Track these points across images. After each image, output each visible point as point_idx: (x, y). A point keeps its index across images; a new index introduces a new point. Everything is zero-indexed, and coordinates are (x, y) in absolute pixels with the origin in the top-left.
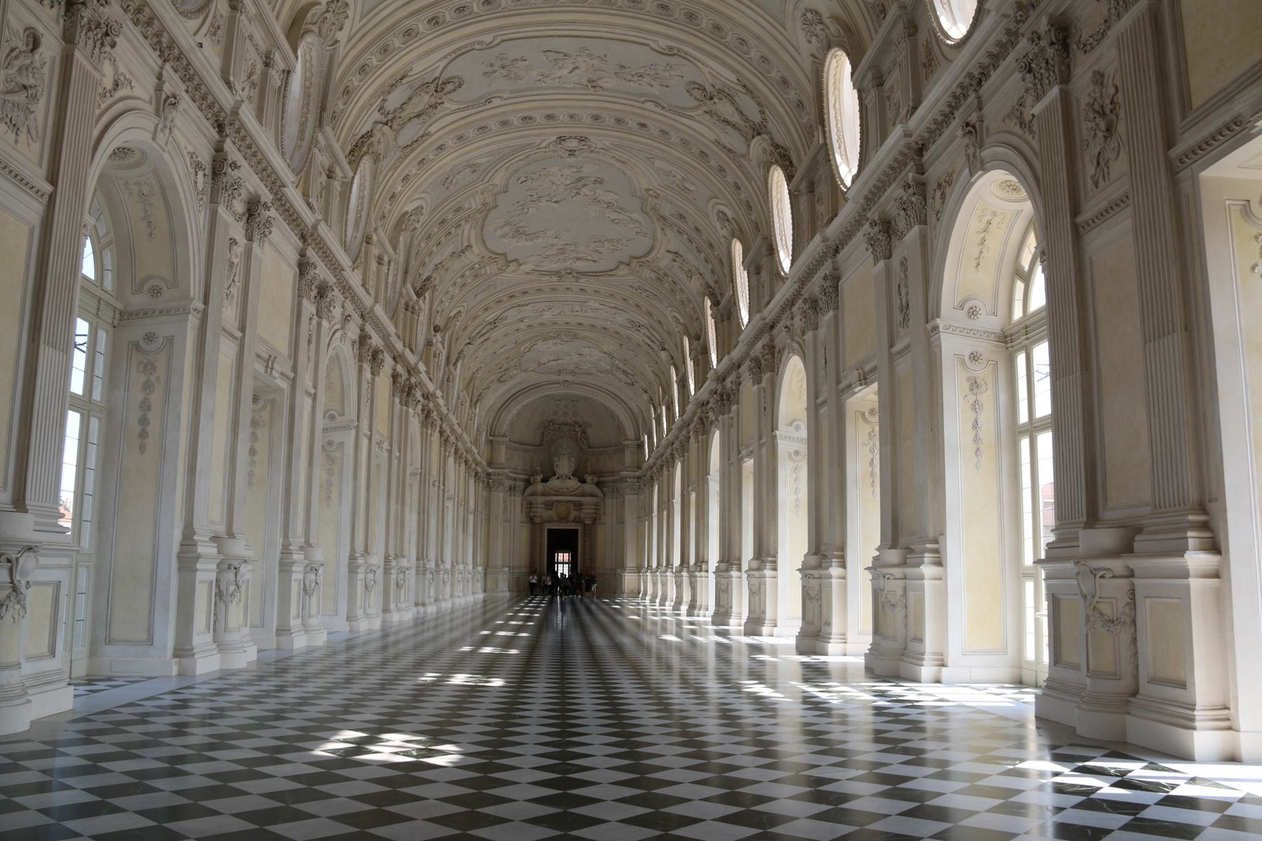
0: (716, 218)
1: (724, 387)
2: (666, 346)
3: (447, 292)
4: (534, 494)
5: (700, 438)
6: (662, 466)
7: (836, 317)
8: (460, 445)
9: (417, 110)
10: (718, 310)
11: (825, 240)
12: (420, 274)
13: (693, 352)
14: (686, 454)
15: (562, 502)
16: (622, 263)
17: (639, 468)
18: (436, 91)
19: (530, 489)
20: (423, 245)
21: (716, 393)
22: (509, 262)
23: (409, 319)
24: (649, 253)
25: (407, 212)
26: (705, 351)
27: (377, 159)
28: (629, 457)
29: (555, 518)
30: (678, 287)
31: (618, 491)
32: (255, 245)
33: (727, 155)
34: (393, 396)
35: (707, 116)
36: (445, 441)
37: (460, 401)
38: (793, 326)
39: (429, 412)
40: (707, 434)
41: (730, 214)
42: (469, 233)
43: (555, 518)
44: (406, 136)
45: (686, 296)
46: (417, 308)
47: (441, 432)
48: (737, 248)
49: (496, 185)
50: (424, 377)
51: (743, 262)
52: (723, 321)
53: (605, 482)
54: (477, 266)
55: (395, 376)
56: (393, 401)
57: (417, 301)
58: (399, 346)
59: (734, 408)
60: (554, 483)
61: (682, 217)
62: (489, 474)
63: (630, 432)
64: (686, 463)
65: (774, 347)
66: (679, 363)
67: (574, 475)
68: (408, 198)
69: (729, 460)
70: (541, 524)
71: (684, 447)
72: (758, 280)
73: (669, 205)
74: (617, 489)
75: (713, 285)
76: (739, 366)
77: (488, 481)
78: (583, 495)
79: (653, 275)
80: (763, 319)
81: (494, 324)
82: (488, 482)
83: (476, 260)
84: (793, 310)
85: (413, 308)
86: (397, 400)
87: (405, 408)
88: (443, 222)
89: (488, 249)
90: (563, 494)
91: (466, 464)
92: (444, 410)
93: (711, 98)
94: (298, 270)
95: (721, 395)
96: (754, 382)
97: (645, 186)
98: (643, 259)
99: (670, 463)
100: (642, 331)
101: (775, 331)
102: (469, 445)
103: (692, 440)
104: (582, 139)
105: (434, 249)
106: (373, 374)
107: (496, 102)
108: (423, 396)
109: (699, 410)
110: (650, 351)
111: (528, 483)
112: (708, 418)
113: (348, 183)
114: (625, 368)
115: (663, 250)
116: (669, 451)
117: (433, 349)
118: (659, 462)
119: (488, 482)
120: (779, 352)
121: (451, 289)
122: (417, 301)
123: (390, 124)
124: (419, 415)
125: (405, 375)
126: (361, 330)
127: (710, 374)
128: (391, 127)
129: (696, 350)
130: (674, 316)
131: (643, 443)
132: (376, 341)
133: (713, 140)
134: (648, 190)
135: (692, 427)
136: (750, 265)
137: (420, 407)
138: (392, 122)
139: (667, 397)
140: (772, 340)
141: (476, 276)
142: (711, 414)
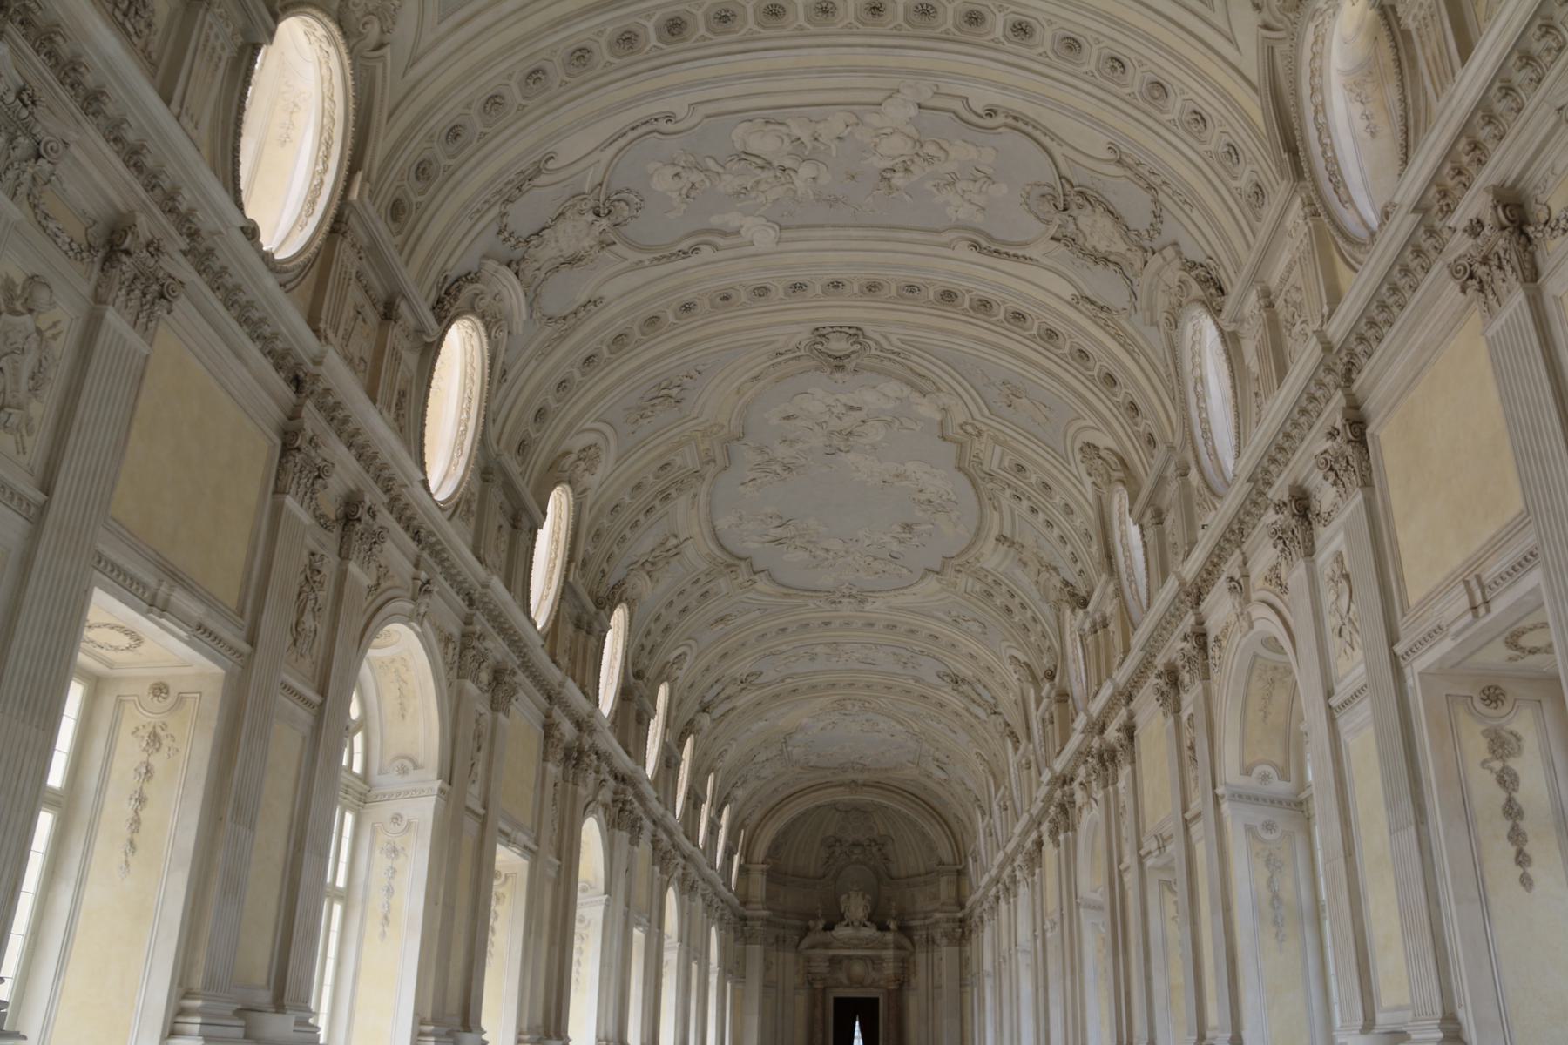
0: (1079, 456)
1: (1103, 740)
2: (1000, 709)
3: (658, 618)
4: (813, 947)
5: (1061, 837)
6: (998, 898)
7: (1369, 504)
8: (691, 870)
9: (568, 252)
10: (1086, 613)
11: (1327, 347)
12: (603, 571)
13: (1045, 702)
14: (1037, 871)
15: (849, 957)
16: (929, 570)
17: (962, 906)
18: (598, 215)
19: (806, 942)
20: (606, 522)
21: (1089, 754)
22: (755, 573)
23: (581, 639)
24: (968, 548)
25: (567, 453)
26: (1063, 697)
27: (492, 322)
28: (945, 888)
29: (845, 981)
30: (1017, 600)
31: (934, 942)
32: (115, 320)
33: (1093, 319)
34: (545, 760)
35: (1059, 249)
36: (661, 857)
37: (692, 801)
38: (1246, 576)
39: (624, 803)
40: (1074, 830)
41: (1104, 440)
42: (684, 516)
43: (845, 981)
44: (553, 302)
45: (1029, 614)
46: (596, 626)
47: (655, 842)
48: (1119, 500)
49: (723, 427)
50: (609, 742)
51: (1130, 511)
52: (1096, 632)
53: (916, 927)
54: (703, 580)
55: (549, 728)
56: (544, 770)
57: (597, 614)
58: (554, 674)
59: (1125, 772)
60: (841, 932)
61: (1021, 468)
62: (744, 919)
63: (946, 853)
64: (1037, 888)
65: (1204, 635)
66: (1020, 733)
67: (869, 920)
68: (571, 425)
69: (1120, 862)
70: (824, 989)
71: (1035, 857)
72: (1161, 536)
73: (998, 449)
74: (933, 938)
75: (1071, 579)
76: (1130, 699)
77: (739, 927)
78: (885, 947)
79: (978, 587)
80: (1182, 584)
81: (745, 682)
82: (743, 931)
83: (704, 566)
84: (1245, 547)
85: (590, 624)
86: (554, 770)
87: (570, 786)
88: (638, 486)
89: (722, 547)
90: (856, 947)
91: (704, 900)
92: (657, 808)
93: (1065, 209)
94: (279, 442)
95: (1101, 756)
96: (1165, 714)
97: (960, 418)
98: (963, 560)
99: (1010, 890)
100: (961, 689)
101: (1203, 605)
102: (709, 871)
103: (1048, 847)
104: (855, 333)
105: (627, 532)
106: (495, 707)
107: (706, 252)
108: (616, 778)
109: (1058, 793)
110: (975, 722)
111: (807, 930)
112: (1074, 803)
113: (432, 344)
114: (937, 754)
115: (992, 541)
116: (1008, 870)
117: (634, 706)
118: (994, 891)
119: (743, 931)
120: (1217, 640)
121: (663, 611)
122: (597, 614)
123: (514, 265)
124: (605, 806)
125: (567, 729)
126: (466, 624)
127: (1080, 722)
128: (517, 274)
129: (1048, 697)
130: (1013, 657)
131: (966, 867)
132: (496, 647)
133: (1069, 298)
134: (961, 427)
135: (1045, 827)
136: (1142, 515)
137: (606, 795)
138: (518, 264)
139: (1002, 789)
140: (1200, 622)
141: (705, 595)
142: (1080, 796)
